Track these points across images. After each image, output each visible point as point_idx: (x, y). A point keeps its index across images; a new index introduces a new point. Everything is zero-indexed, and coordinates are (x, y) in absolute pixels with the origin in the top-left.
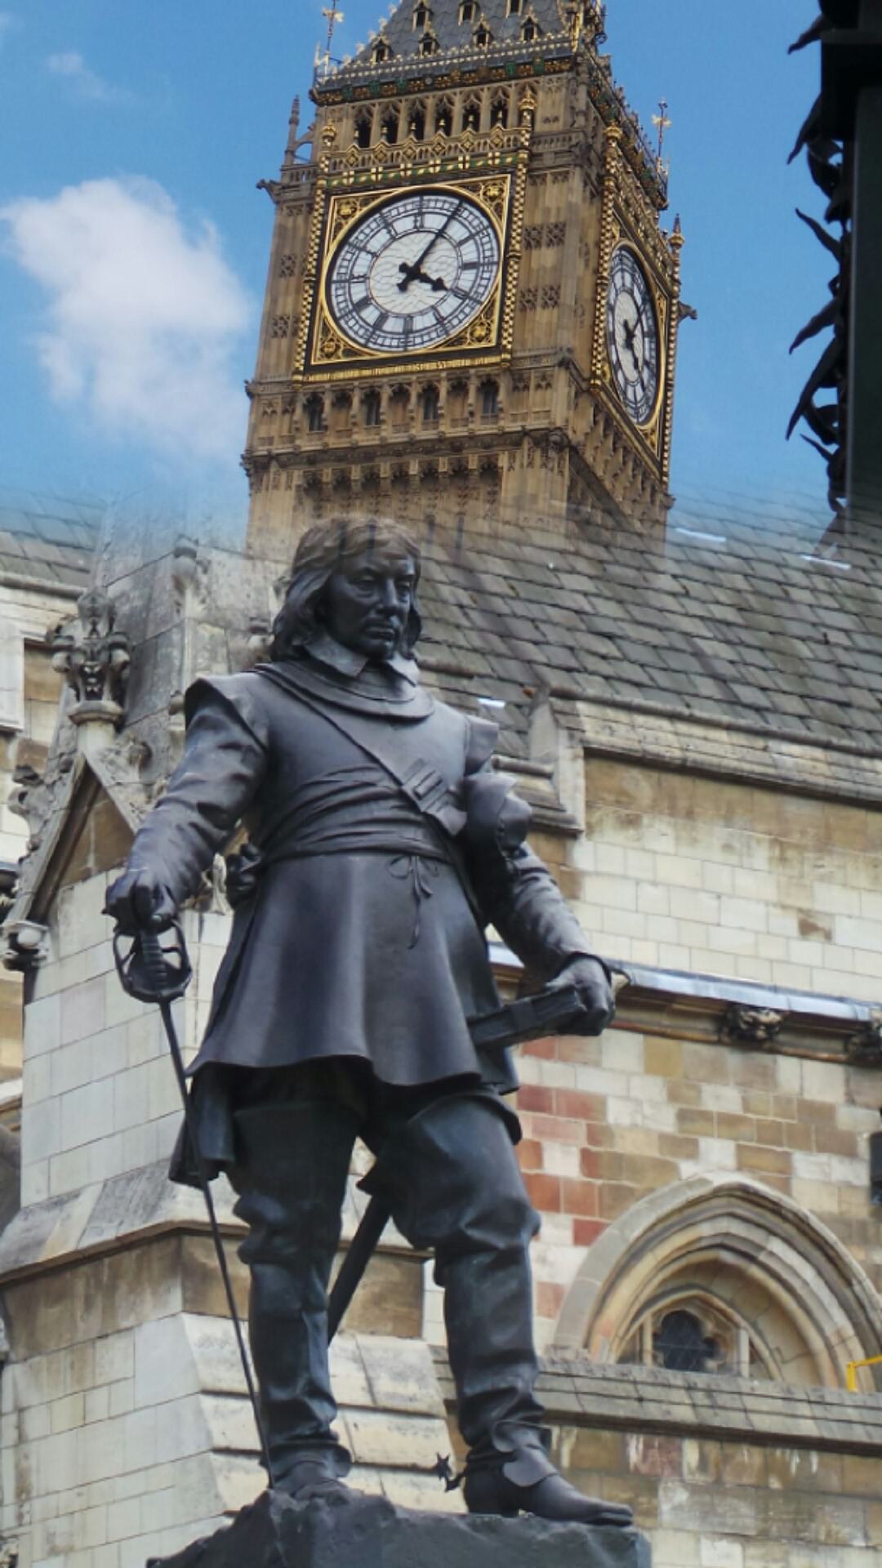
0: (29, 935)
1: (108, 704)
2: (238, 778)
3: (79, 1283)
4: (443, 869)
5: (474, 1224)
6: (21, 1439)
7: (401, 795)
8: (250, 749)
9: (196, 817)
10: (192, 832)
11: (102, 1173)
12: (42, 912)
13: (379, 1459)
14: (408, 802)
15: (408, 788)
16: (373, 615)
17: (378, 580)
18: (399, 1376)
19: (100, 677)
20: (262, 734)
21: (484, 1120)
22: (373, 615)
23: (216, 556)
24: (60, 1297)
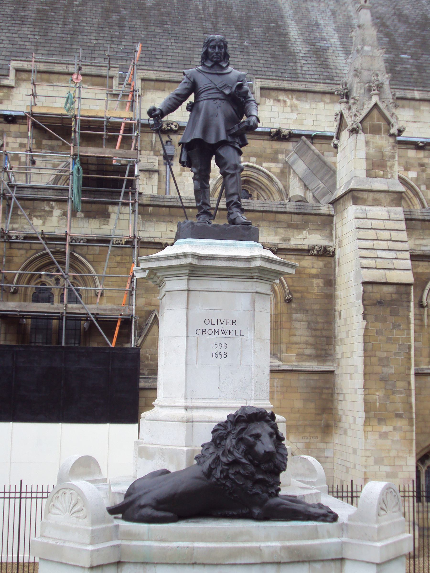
0: (336, 142)
1: (345, 100)
2: (186, 89)
3: (341, 201)
4: (225, 102)
5: (227, 169)
6: (336, 229)
7: (216, 88)
8: (189, 83)
9: (175, 96)
10: (173, 99)
11: (344, 182)
12: (338, 138)
13: (390, 228)
14: (218, 90)
15: (217, 87)
16: (214, 54)
17: (214, 47)
18: (395, 214)
19: (343, 95)
20: (192, 80)
21: (231, 150)
22: (214, 54)
23: (362, 71)
24: (340, 204)
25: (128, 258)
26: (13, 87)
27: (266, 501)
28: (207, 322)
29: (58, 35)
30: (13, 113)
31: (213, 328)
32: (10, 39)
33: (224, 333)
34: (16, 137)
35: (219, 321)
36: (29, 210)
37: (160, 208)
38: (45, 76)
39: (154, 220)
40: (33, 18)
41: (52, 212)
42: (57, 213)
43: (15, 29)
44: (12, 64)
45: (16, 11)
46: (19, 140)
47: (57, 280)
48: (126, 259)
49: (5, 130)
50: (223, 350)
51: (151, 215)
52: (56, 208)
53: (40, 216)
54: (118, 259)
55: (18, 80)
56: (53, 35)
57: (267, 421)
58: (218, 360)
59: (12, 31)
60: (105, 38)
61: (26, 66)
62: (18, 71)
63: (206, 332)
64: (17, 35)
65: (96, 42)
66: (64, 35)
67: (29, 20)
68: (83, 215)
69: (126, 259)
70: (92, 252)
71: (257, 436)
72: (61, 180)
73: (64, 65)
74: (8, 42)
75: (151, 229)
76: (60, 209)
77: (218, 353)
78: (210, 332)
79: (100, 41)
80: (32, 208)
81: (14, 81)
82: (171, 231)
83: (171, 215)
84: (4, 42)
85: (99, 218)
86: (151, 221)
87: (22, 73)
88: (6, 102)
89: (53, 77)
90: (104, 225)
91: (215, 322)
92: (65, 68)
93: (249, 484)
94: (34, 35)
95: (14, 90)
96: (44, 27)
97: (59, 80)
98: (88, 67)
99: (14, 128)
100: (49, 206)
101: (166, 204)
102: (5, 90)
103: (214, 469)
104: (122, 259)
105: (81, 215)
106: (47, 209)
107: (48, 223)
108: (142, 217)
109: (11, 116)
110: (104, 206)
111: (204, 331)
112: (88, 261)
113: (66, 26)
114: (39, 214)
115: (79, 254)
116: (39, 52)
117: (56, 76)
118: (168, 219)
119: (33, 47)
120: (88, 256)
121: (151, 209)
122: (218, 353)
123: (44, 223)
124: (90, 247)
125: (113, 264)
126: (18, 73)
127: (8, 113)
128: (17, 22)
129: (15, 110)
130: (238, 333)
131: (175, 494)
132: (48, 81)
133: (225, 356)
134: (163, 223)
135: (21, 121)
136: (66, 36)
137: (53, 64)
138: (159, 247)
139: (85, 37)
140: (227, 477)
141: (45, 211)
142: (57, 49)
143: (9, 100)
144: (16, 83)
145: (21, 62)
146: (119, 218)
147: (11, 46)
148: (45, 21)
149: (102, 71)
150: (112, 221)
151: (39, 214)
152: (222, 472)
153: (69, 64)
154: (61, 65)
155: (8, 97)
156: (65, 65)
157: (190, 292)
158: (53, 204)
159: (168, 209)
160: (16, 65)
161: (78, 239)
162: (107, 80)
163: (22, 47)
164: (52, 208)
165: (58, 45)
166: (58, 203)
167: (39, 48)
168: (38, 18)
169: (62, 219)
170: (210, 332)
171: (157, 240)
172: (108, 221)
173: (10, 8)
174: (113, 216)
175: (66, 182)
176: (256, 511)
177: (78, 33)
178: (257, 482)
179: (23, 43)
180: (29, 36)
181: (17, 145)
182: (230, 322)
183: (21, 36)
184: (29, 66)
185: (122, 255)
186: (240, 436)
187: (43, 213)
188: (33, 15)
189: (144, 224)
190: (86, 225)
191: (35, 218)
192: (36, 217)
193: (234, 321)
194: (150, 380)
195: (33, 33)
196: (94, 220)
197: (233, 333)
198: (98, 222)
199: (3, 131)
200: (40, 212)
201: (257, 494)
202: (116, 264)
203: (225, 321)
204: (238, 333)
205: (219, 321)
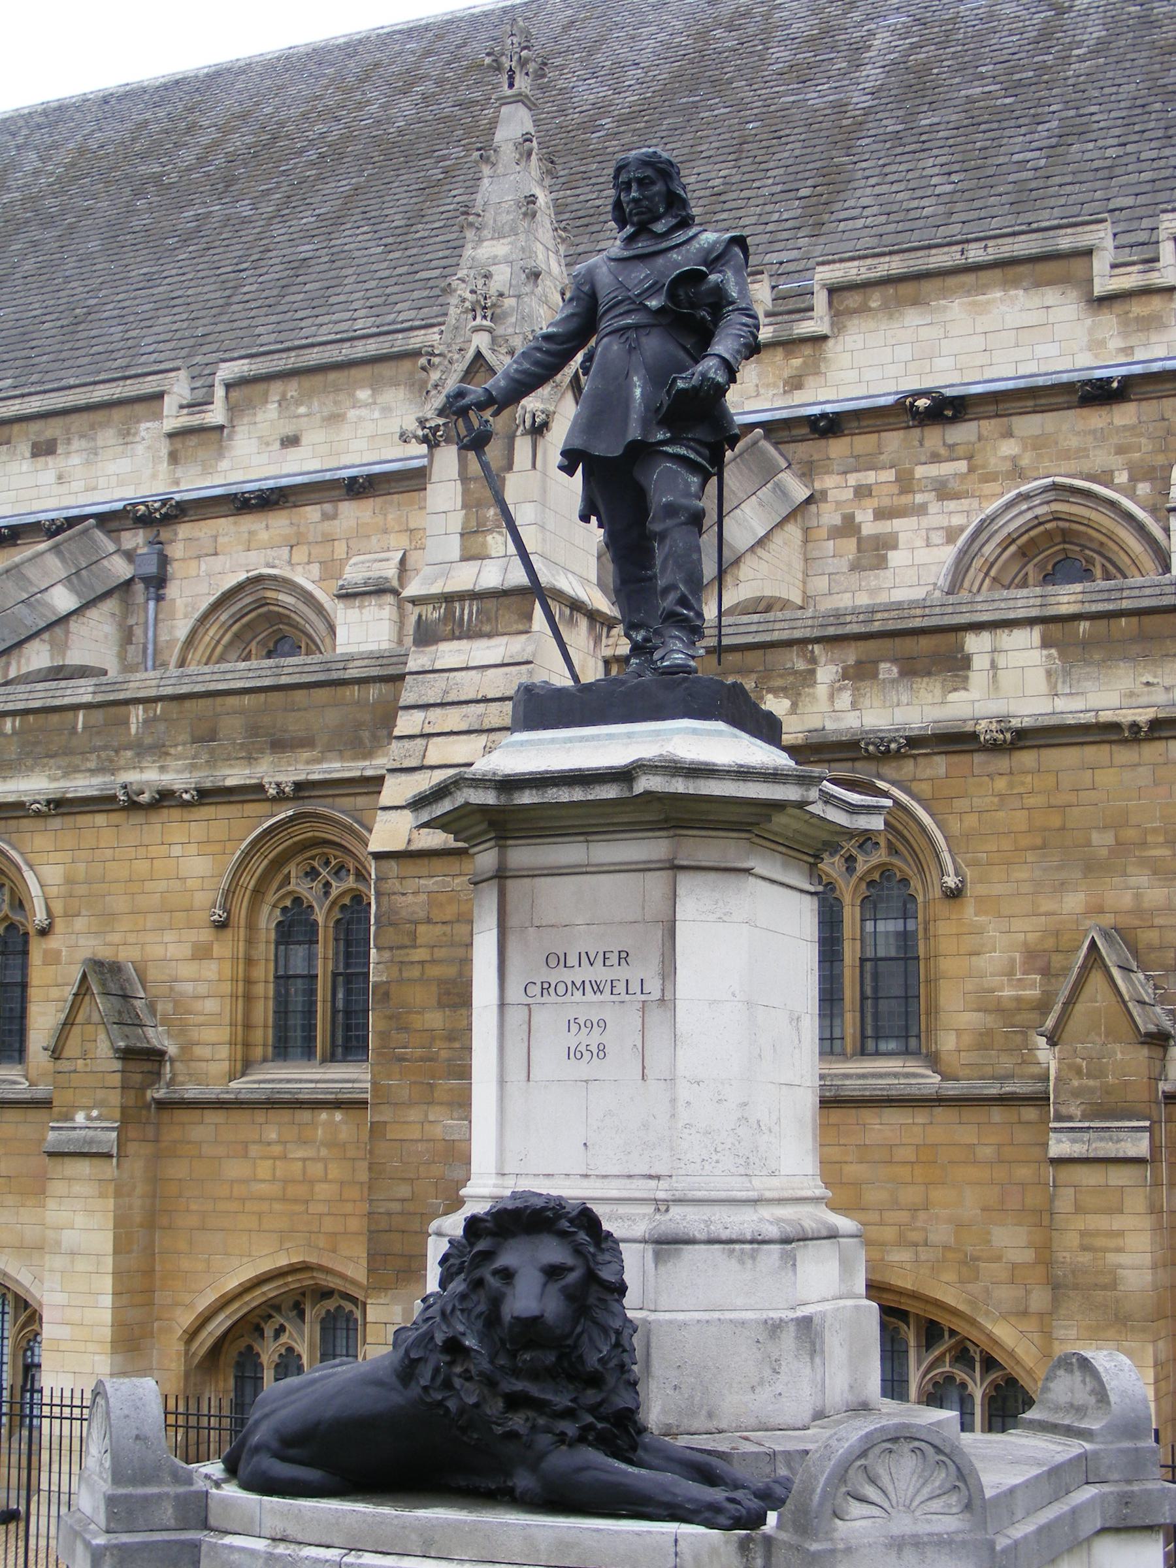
25: (1029, 778)
26: (825, 338)
27: (542, 1456)
28: (553, 963)
29: (1016, 158)
30: (829, 408)
31: (568, 976)
32: (882, 199)
33: (597, 989)
34: (845, 473)
35: (584, 956)
36: (754, 676)
37: (1112, 621)
38: (907, 289)
39: (1097, 657)
40: (951, 126)
41: (813, 672)
42: (826, 673)
43: (902, 167)
44: (817, 277)
45: (909, 118)
46: (853, 479)
47: (850, 860)
48: (1023, 783)
49: (815, 457)
50: (594, 1039)
51: (1086, 644)
52: (823, 660)
53: (784, 689)
54: (1001, 784)
55: (838, 315)
56: (1001, 160)
57: (563, 1234)
58: (583, 1069)
59: (891, 178)
60: (1147, 135)
61: (855, 271)
62: (834, 290)
63: (552, 990)
64: (902, 186)
65: (1120, 151)
66: (1029, 155)
67: (941, 134)
68: (895, 670)
69: (1023, 783)
70: (928, 773)
71: (507, 1275)
72: (972, 570)
73: (954, 248)
74: (875, 210)
75: (1088, 685)
76: (832, 661)
77: (582, 1048)
78: (561, 989)
79: (1129, 148)
80: (761, 668)
81: (827, 319)
82: (1148, 684)
83: (1143, 637)
84: (866, 212)
85: (940, 672)
86: (1087, 663)
87: (846, 294)
88: (810, 382)
89: (927, 286)
90: (955, 690)
91: (572, 960)
92: (958, 256)
93: (494, 1408)
94: (949, 174)
95: (831, 343)
96: (978, 145)
97: (944, 293)
98: (1023, 237)
99: (837, 448)
100: (805, 656)
101: (1125, 604)
102: (807, 350)
103: (419, 1360)
104: (1011, 785)
105: (890, 670)
106: (801, 665)
107: (805, 706)
108: (1062, 655)
109: (824, 416)
110: (951, 637)
111: (545, 988)
112: (919, 800)
113: (1040, 128)
114: (779, 682)
115: (893, 783)
116: (954, 218)
117: (937, 283)
118: (1136, 649)
119: (941, 209)
120: (916, 787)
121: (1084, 626)
122: (582, 1048)
123: (794, 705)
124: (920, 760)
125: (988, 800)
126: (835, 296)
127: (816, 410)
128: (907, 149)
129: (834, 398)
130: (635, 987)
131: (318, 1424)
132: (916, 302)
133: (601, 1054)
134: (1121, 664)
135: (855, 424)
136: (1037, 154)
137: (926, 252)
138: (1115, 737)
139: (1091, 145)
140: (447, 1385)
141: (796, 672)
142: (1004, 199)
143: (817, 373)
144: (832, 324)
145: (843, 265)
146: (994, 666)
147: (883, 219)
148: (983, 127)
149: (1060, 241)
150: (978, 676)
151: (779, 682)
152: (437, 1370)
153: (968, 241)
154: (946, 249)
155: (814, 368)
156: (959, 248)
157: (509, 882)
158: (817, 649)
159: (1135, 620)
160: (828, 275)
161: (882, 739)
162: (1077, 265)
163: (913, 214)
164: (813, 660)
165: (1010, 187)
166: (828, 647)
167: (959, 206)
168: (966, 122)
169: (840, 689)
170: (561, 989)
171: (1106, 717)
172: (967, 678)
173: (895, 113)
174: (980, 662)
175: (987, 574)
176: (523, 1481)
177: (1070, 140)
178: (514, 1402)
179: (915, 204)
180: (934, 181)
181: (849, 494)
182: (614, 959)
183: (912, 185)
184: (863, 270)
185: (1011, 773)
186: (477, 1274)
187: (791, 679)
188: (954, 117)
189: (1067, 673)
190: (904, 699)
191: (770, 696)
192: (775, 691)
193: (624, 955)
194: (1086, 1136)
195: (946, 169)
196: (926, 680)
197: (620, 988)
198: (938, 685)
199: (811, 462)
200: (781, 676)
201: (512, 1435)
202: (996, 800)
203: (601, 956)
204: (635, 987)
205: (584, 956)
